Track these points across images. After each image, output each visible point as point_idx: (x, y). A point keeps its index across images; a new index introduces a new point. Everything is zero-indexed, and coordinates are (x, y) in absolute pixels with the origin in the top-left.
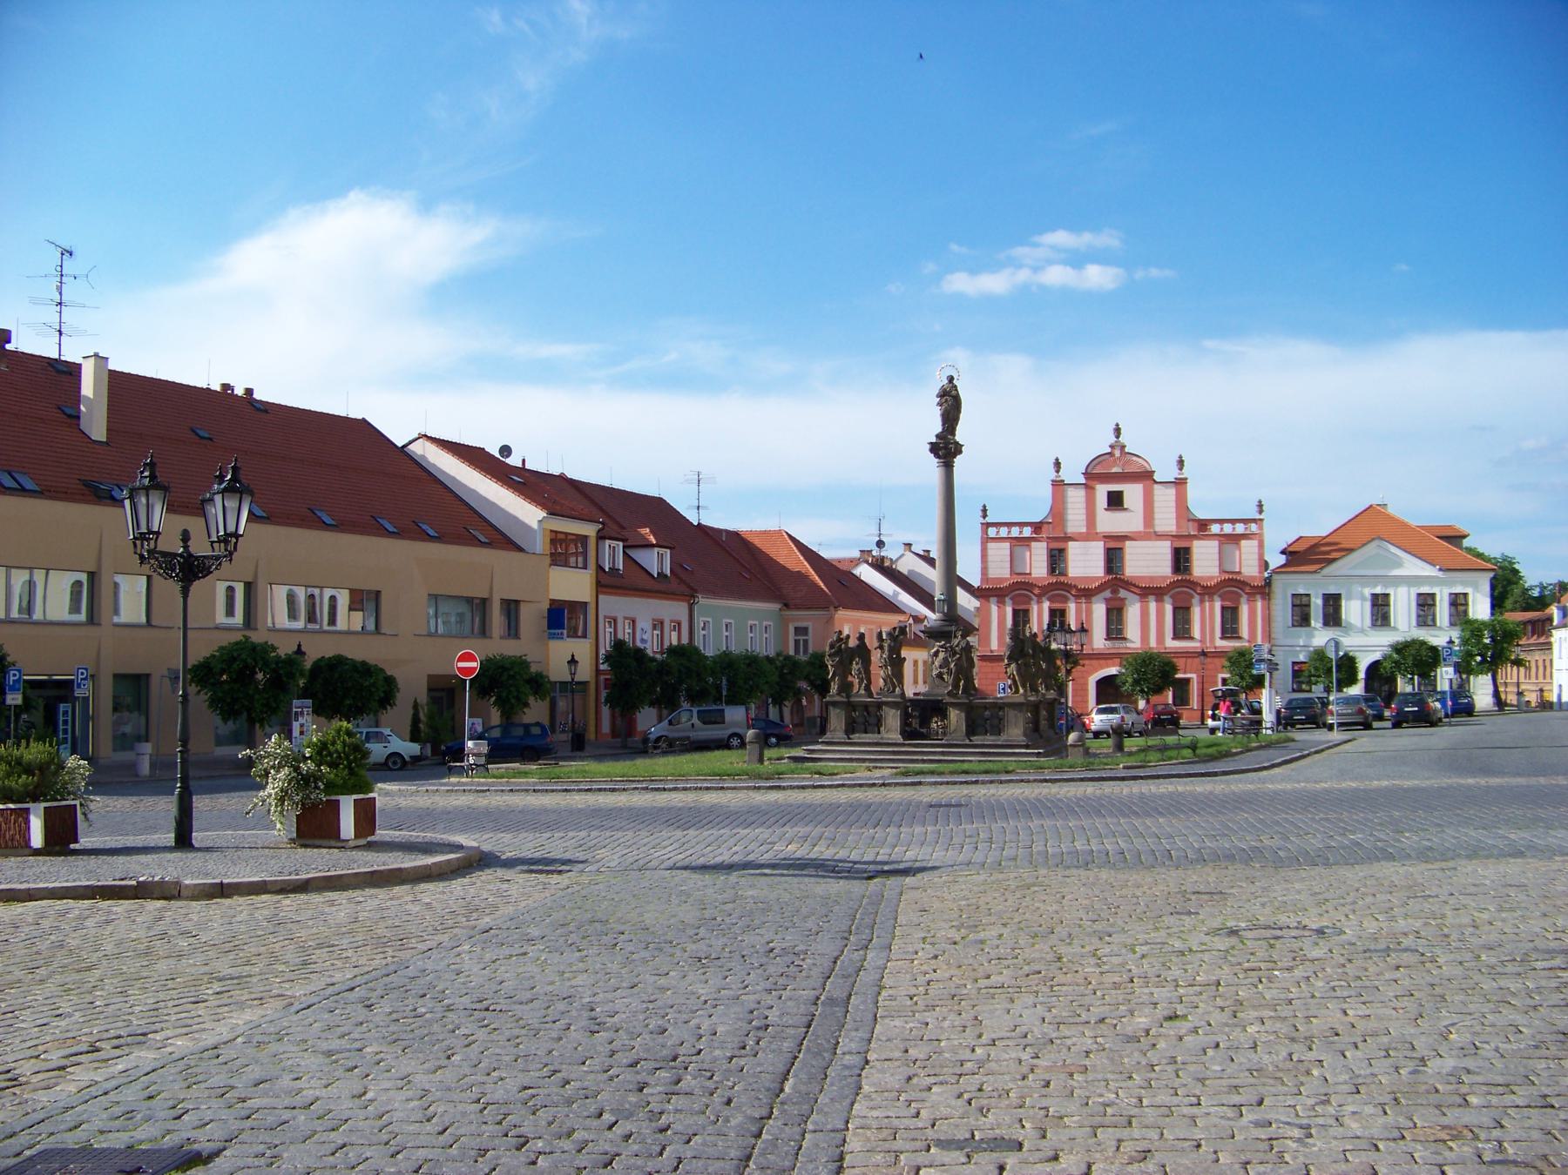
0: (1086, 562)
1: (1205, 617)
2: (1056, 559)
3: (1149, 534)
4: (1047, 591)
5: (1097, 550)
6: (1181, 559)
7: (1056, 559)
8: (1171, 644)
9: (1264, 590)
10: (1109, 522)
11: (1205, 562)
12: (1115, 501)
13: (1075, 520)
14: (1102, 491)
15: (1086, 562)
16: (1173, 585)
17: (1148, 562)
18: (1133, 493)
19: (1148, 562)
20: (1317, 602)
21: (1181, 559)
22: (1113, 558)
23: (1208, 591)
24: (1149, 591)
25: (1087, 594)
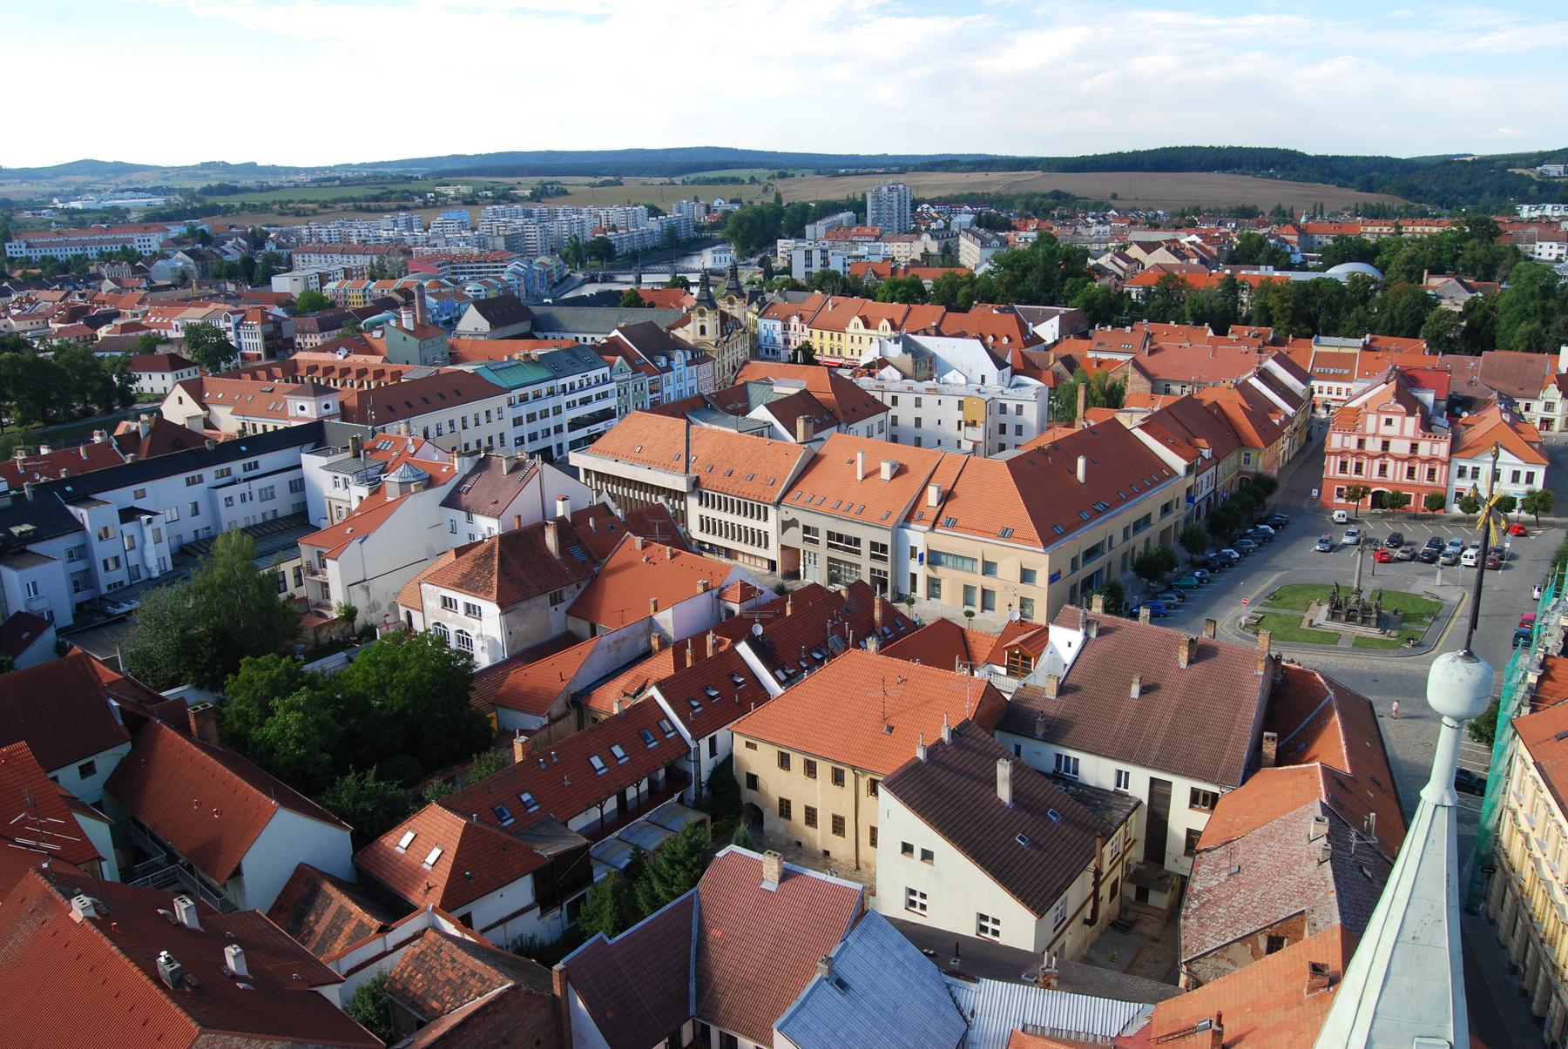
0: (1373, 446)
1: (1421, 471)
2: (1361, 443)
3: (1401, 437)
4: (1355, 455)
5: (1379, 441)
6: (1414, 447)
7: (1361, 443)
8: (1405, 480)
9: (1449, 463)
10: (1385, 430)
11: (1424, 449)
12: (1389, 422)
13: (1370, 428)
14: (1383, 418)
15: (1373, 446)
16: (1407, 459)
17: (1400, 447)
18: (1396, 420)
19: (1400, 447)
20: (1469, 470)
21: (1414, 447)
22: (1385, 445)
23: (1423, 461)
24: (1397, 459)
25: (1372, 457)
